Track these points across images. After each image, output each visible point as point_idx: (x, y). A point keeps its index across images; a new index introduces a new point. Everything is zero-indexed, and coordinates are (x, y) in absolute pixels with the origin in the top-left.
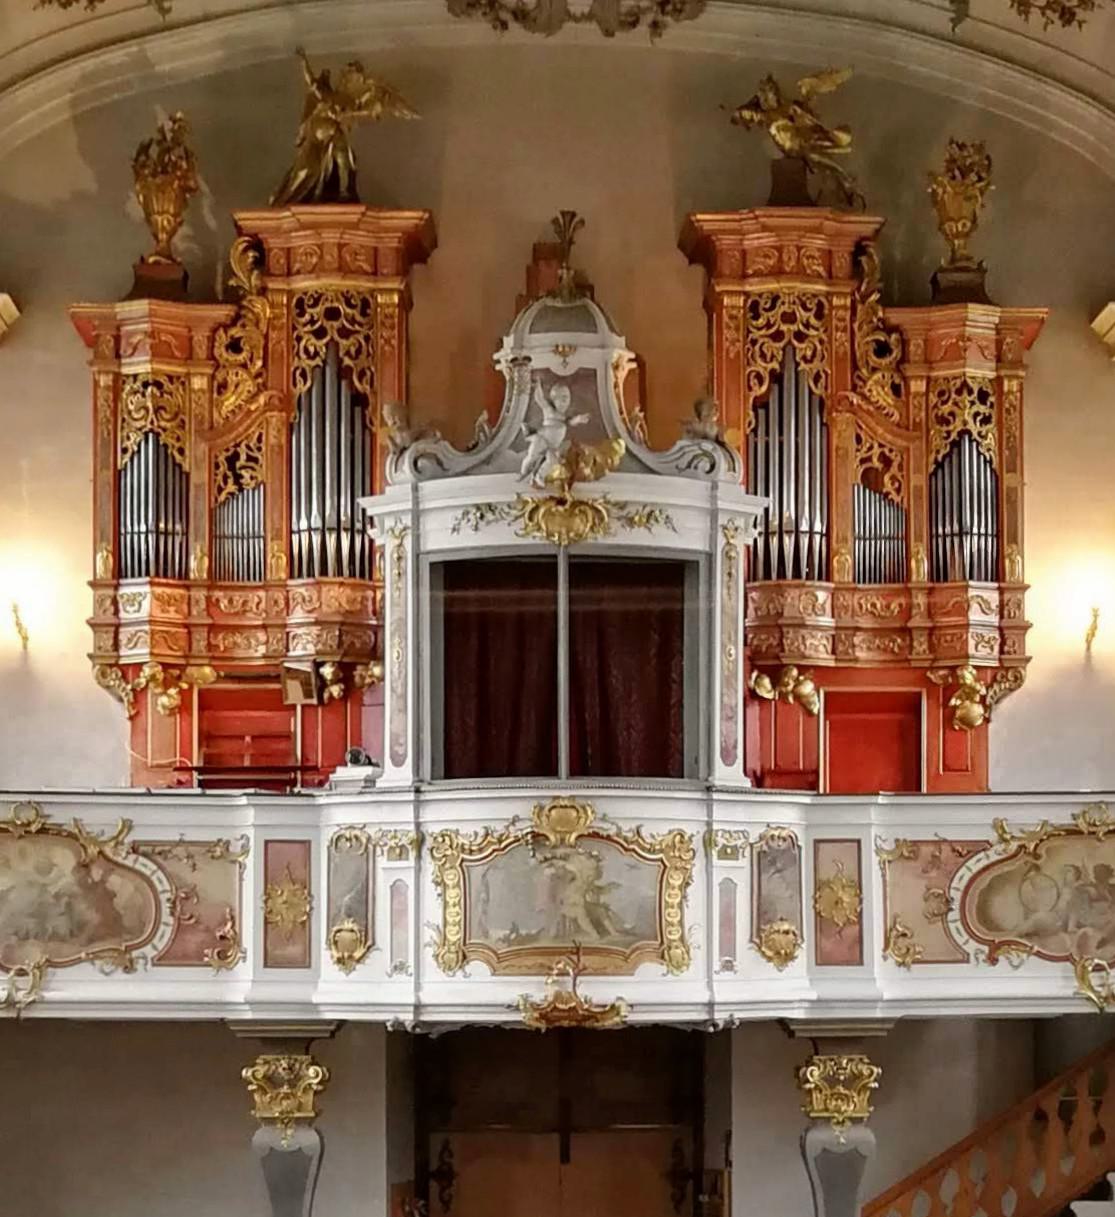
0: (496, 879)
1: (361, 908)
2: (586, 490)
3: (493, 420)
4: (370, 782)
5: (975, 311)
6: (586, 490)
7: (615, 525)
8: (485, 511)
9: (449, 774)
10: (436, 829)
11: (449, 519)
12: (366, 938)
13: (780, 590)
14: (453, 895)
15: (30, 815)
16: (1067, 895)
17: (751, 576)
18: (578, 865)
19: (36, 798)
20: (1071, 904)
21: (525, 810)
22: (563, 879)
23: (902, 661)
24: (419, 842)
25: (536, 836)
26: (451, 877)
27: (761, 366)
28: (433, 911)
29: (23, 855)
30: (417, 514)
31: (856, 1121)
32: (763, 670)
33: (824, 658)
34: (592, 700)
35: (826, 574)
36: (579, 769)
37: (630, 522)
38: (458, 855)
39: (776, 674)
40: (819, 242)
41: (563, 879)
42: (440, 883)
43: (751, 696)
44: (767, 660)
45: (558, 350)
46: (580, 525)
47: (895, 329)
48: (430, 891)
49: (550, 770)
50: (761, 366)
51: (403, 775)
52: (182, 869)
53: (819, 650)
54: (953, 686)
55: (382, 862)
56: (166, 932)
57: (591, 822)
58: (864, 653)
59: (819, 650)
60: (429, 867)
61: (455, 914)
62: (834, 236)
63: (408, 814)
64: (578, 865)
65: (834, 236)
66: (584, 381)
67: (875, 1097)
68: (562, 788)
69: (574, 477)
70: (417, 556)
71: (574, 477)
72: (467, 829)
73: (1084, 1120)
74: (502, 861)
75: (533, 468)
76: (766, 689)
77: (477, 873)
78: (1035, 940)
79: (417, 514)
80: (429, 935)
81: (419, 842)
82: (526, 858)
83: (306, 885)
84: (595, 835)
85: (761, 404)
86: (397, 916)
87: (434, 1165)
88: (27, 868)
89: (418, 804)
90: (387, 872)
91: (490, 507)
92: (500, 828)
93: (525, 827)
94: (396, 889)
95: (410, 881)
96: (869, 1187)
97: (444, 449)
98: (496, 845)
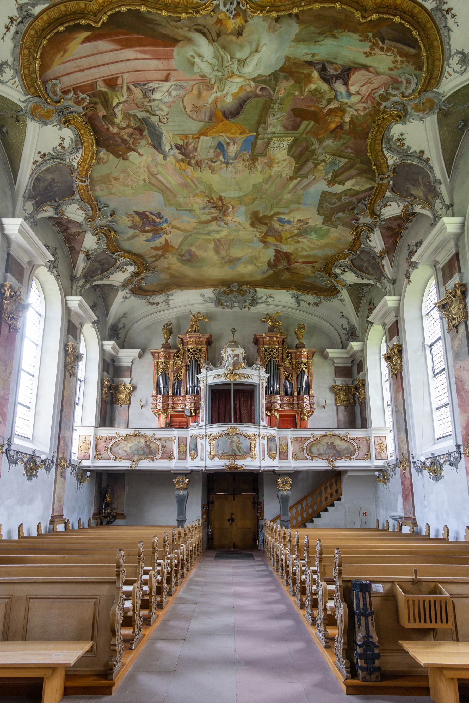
0: (220, 442)
1: (195, 449)
2: (237, 371)
3: (221, 363)
4: (197, 425)
5: (303, 350)
6: (237, 371)
7: (242, 378)
8: (219, 376)
9: (212, 423)
10: (209, 433)
11: (212, 378)
12: (196, 455)
13: (271, 396)
14: (212, 445)
15: (136, 432)
16: (325, 447)
17: (266, 394)
18: (235, 439)
19: (138, 429)
20: (326, 449)
21: (225, 429)
22: (232, 442)
23: (293, 409)
24: (206, 436)
25: (228, 434)
26: (212, 442)
27: (267, 359)
28: (208, 448)
29: (135, 440)
30: (206, 377)
31: (288, 490)
32: (268, 410)
33: (279, 408)
34: (238, 413)
35: (279, 394)
36: (236, 421)
37: (245, 377)
38: (213, 438)
39: (271, 411)
40: (277, 339)
41: (232, 442)
42: (210, 443)
43: (267, 415)
44: (269, 408)
45: (233, 351)
46: (236, 378)
47: (290, 353)
48: (208, 445)
49: (230, 421)
50: (267, 359)
51: (203, 424)
52: (164, 442)
53: (278, 407)
54: (302, 413)
55: (199, 440)
56: (160, 454)
57: (237, 431)
58: (286, 408)
59: (278, 407)
60: (208, 440)
61: (212, 449)
62: (279, 338)
63: (204, 430)
64: (235, 439)
65: (279, 338)
66: (237, 355)
67: (291, 485)
68: (232, 425)
69: (234, 369)
70: (206, 385)
71: (234, 369)
72: (215, 433)
73: (329, 491)
74: (221, 438)
75: (227, 368)
76: (269, 414)
77: (216, 441)
78: (320, 456)
79: (206, 377)
80: (208, 453)
81: (206, 436)
82: (225, 438)
83: (186, 445)
84: (238, 434)
85: (267, 365)
86: (202, 450)
87: (211, 500)
88: (136, 442)
89: (206, 428)
90: (200, 441)
91: (219, 375)
92: (221, 432)
93: (225, 432)
94: (202, 445)
95: (204, 443)
96: (291, 503)
97: (212, 367)
98: (220, 436)
